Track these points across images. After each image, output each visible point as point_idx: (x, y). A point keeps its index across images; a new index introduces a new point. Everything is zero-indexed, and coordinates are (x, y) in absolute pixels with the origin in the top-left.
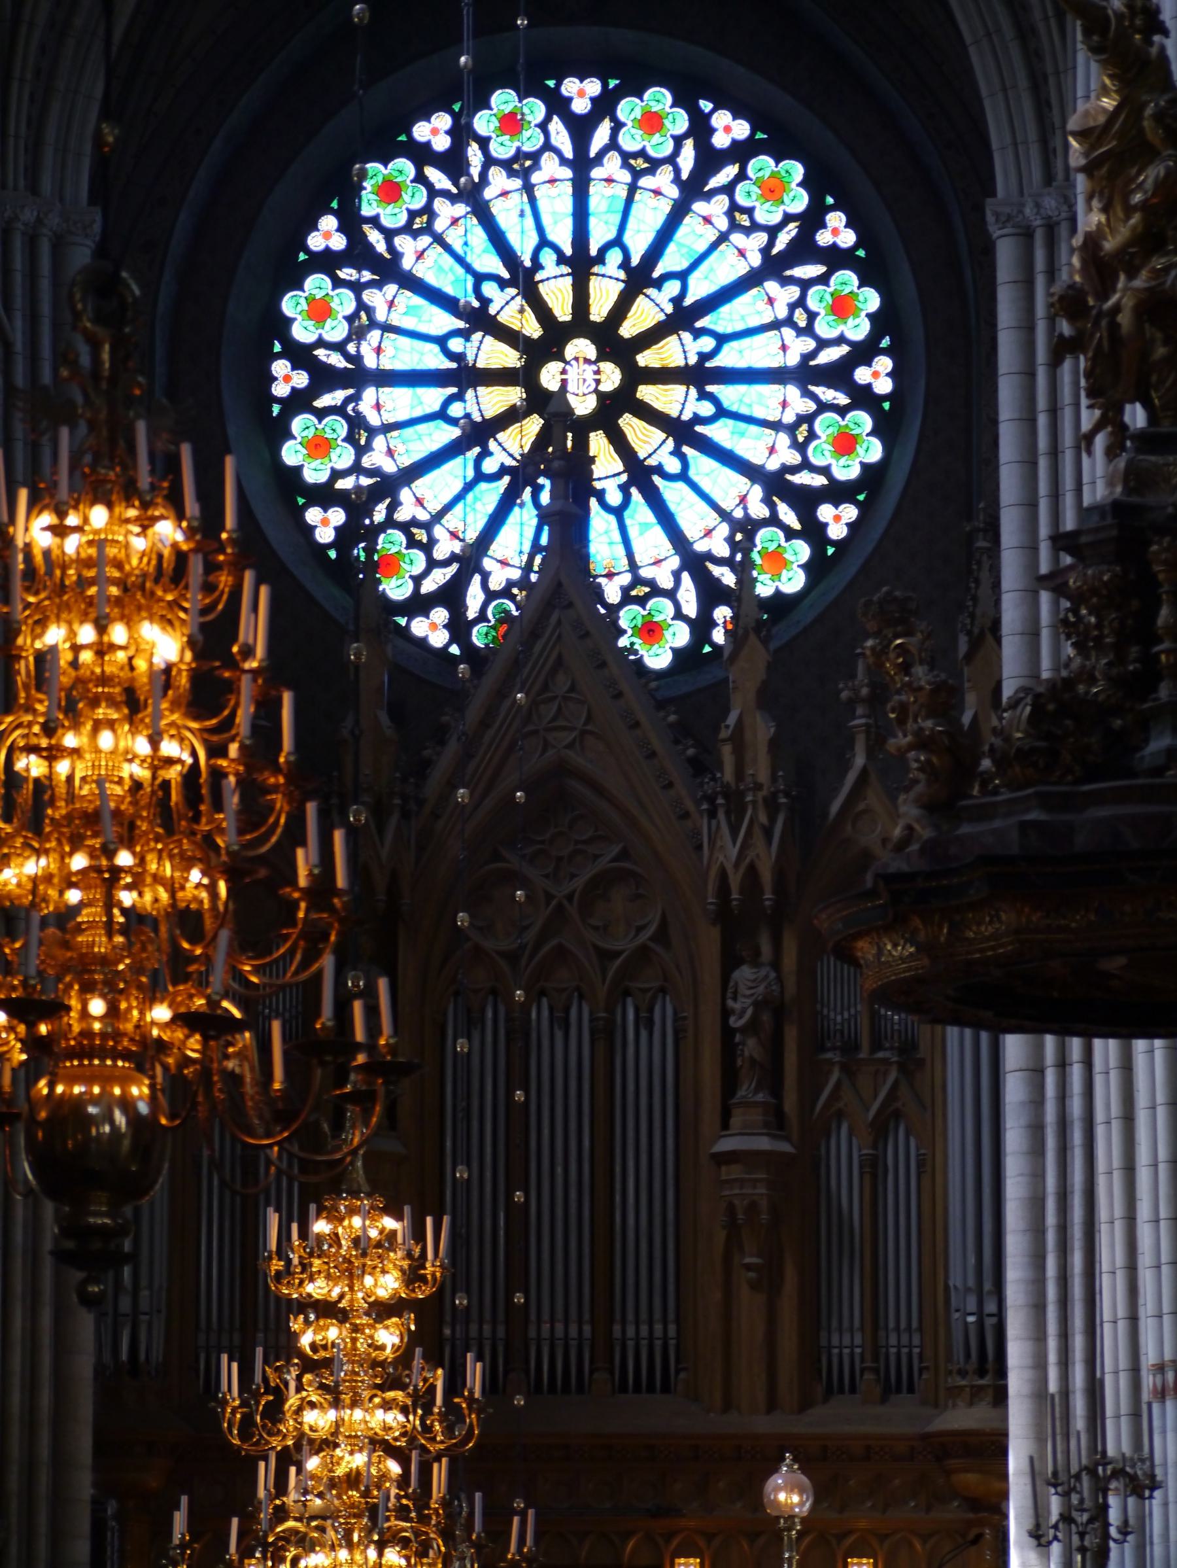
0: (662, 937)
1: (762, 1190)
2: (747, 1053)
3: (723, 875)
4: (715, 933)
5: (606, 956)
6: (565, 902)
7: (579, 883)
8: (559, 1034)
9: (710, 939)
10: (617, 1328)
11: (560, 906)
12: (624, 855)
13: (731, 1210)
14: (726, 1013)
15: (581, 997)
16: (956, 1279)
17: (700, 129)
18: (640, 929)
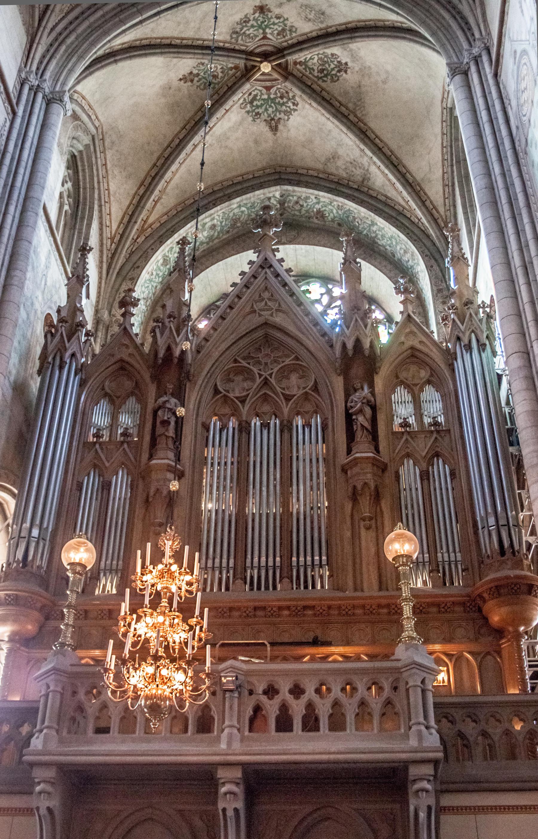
0: (315, 388)
1: (369, 476)
2: (359, 423)
3: (344, 345)
4: (341, 379)
5: (288, 398)
6: (268, 377)
7: (275, 370)
8: (265, 432)
9: (339, 383)
10: (294, 559)
11: (266, 378)
12: (297, 358)
13: (355, 487)
14: (347, 410)
15: (276, 417)
16: (480, 512)
17: (329, 292)
18: (304, 388)
